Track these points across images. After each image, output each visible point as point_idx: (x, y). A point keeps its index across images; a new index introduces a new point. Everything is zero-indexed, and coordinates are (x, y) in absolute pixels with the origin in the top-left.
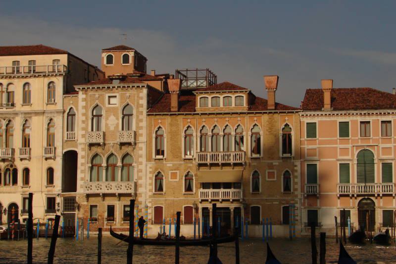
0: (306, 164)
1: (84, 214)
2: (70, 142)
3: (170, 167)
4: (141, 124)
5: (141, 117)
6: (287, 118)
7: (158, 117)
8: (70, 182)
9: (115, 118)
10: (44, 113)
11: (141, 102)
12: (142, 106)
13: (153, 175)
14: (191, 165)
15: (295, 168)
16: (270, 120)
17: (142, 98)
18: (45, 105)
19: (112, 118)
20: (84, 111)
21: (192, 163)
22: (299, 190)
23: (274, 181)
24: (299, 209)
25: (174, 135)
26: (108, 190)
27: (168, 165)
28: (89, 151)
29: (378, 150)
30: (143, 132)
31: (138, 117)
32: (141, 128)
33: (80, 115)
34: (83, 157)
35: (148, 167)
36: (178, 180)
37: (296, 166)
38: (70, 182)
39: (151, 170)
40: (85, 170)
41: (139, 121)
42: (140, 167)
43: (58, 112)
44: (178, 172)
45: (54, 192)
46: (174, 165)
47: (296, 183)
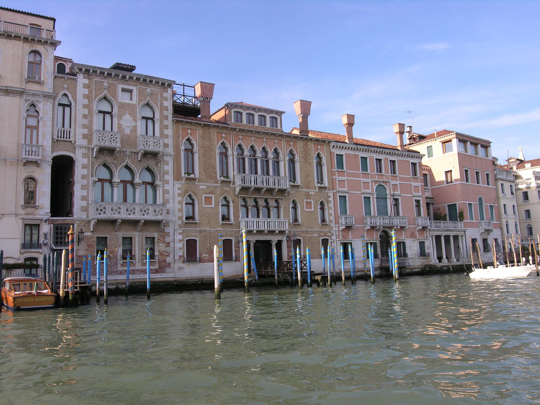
0: (338, 195)
1: (86, 250)
2: (62, 143)
3: (203, 189)
4: (166, 132)
5: (165, 122)
6: (319, 147)
7: (187, 126)
8: (61, 202)
9: (131, 119)
10: (21, 93)
11: (165, 104)
12: (167, 109)
13: (183, 199)
14: (228, 189)
15: (329, 199)
16: (305, 147)
17: (166, 100)
18: (24, 83)
19: (127, 117)
20: (86, 102)
21: (229, 187)
22: (334, 221)
23: (312, 212)
24: (335, 241)
25: (207, 151)
26: (144, 215)
27: (201, 187)
28: (94, 160)
29: (390, 186)
30: (170, 141)
31: (161, 122)
32: (167, 136)
33: (80, 106)
34: (84, 166)
35: (176, 188)
36: (213, 206)
37: (329, 197)
38: (61, 202)
39: (180, 192)
40: (88, 185)
41: (164, 127)
42: (167, 187)
43: (46, 96)
44: (213, 196)
45: (37, 217)
46: (208, 187)
47: (330, 215)
